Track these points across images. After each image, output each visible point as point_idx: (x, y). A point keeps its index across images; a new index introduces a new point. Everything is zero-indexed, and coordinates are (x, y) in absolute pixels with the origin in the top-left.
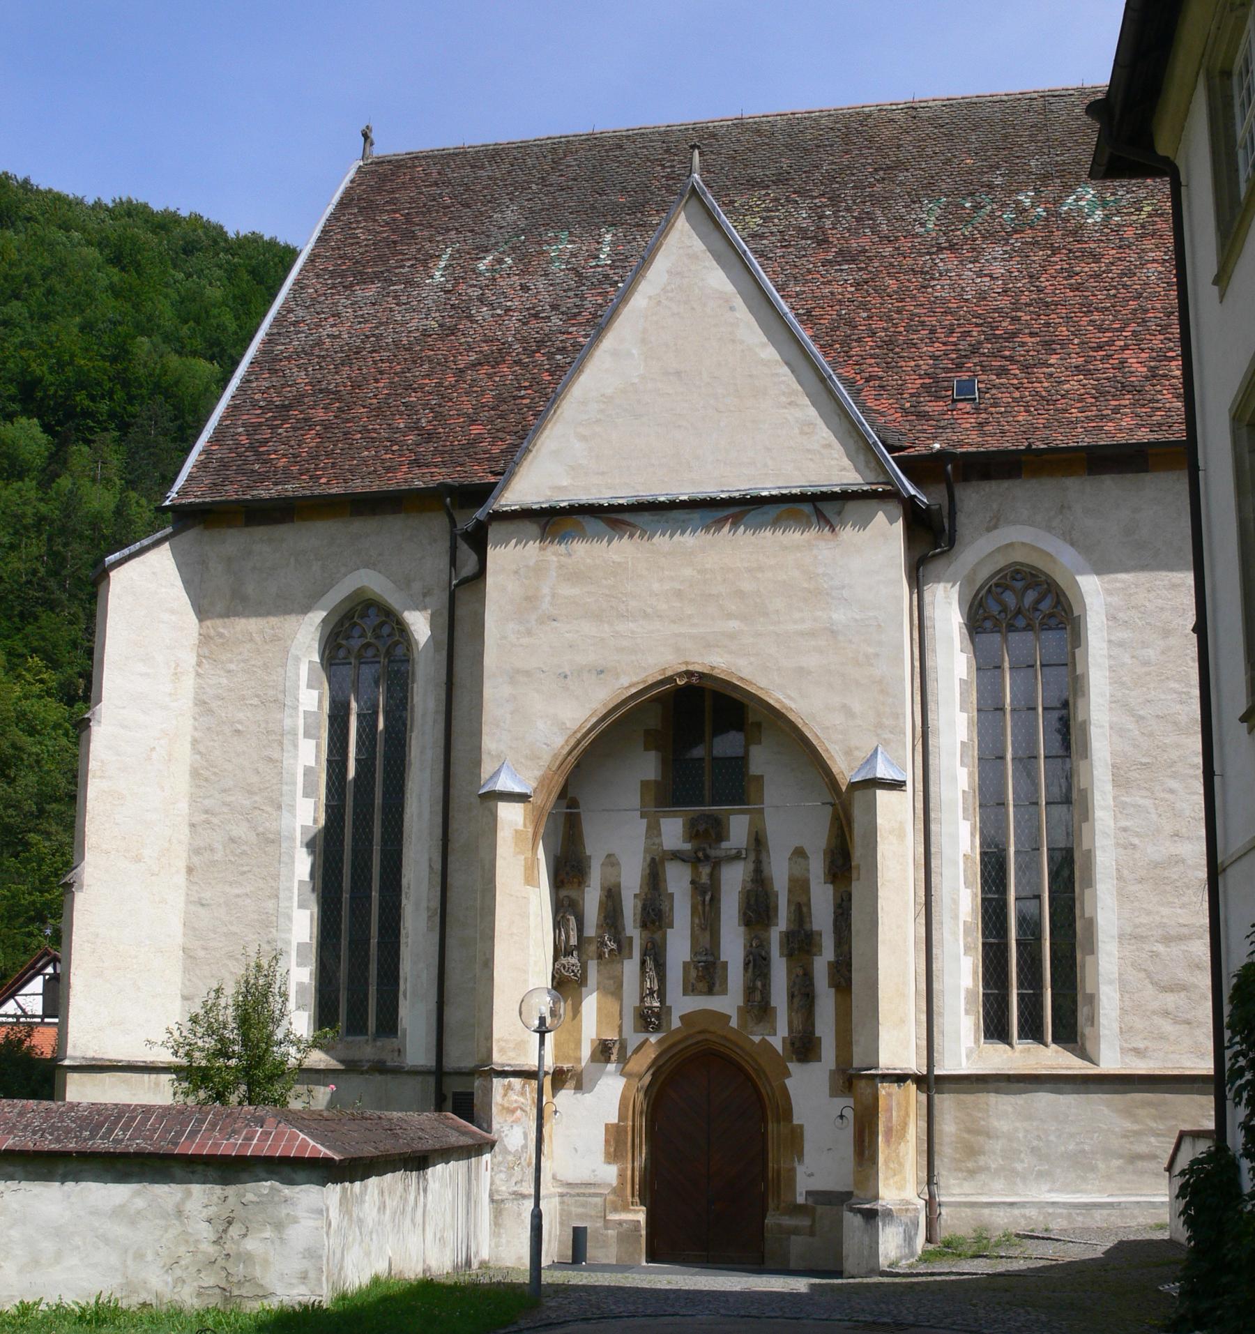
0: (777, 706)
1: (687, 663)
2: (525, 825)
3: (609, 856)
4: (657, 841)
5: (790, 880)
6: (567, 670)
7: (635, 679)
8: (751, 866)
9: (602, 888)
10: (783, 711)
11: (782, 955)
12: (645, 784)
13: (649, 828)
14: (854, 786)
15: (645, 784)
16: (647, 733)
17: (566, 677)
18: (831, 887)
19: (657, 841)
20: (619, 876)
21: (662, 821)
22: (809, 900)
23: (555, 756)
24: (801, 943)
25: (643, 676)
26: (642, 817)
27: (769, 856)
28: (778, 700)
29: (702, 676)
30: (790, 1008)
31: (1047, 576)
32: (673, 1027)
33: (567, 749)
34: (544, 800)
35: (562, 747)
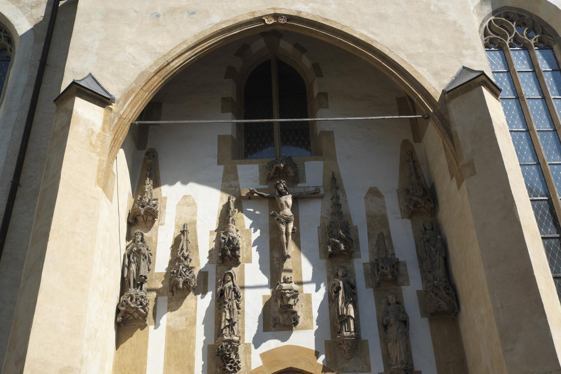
0: (363, 39)
1: (274, 9)
2: (103, 129)
3: (185, 197)
4: (233, 183)
5: (368, 216)
6: (159, 10)
7: (225, 18)
8: (328, 203)
9: (177, 226)
10: (369, 42)
11: (368, 285)
12: (221, 138)
13: (226, 172)
14: (450, 94)
15: (221, 138)
16: (224, 100)
17: (158, 16)
18: (408, 222)
19: (233, 183)
20: (195, 214)
21: (239, 167)
22: (389, 232)
23: (142, 74)
24: (386, 273)
25: (233, 16)
26: (219, 163)
27: (345, 195)
28: (362, 35)
29: (290, 18)
30: (384, 341)
31: (531, 15)
32: (253, 367)
33: (156, 68)
34: (127, 110)
35: (151, 66)
